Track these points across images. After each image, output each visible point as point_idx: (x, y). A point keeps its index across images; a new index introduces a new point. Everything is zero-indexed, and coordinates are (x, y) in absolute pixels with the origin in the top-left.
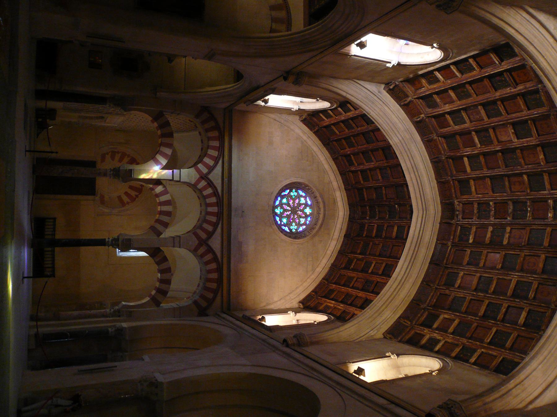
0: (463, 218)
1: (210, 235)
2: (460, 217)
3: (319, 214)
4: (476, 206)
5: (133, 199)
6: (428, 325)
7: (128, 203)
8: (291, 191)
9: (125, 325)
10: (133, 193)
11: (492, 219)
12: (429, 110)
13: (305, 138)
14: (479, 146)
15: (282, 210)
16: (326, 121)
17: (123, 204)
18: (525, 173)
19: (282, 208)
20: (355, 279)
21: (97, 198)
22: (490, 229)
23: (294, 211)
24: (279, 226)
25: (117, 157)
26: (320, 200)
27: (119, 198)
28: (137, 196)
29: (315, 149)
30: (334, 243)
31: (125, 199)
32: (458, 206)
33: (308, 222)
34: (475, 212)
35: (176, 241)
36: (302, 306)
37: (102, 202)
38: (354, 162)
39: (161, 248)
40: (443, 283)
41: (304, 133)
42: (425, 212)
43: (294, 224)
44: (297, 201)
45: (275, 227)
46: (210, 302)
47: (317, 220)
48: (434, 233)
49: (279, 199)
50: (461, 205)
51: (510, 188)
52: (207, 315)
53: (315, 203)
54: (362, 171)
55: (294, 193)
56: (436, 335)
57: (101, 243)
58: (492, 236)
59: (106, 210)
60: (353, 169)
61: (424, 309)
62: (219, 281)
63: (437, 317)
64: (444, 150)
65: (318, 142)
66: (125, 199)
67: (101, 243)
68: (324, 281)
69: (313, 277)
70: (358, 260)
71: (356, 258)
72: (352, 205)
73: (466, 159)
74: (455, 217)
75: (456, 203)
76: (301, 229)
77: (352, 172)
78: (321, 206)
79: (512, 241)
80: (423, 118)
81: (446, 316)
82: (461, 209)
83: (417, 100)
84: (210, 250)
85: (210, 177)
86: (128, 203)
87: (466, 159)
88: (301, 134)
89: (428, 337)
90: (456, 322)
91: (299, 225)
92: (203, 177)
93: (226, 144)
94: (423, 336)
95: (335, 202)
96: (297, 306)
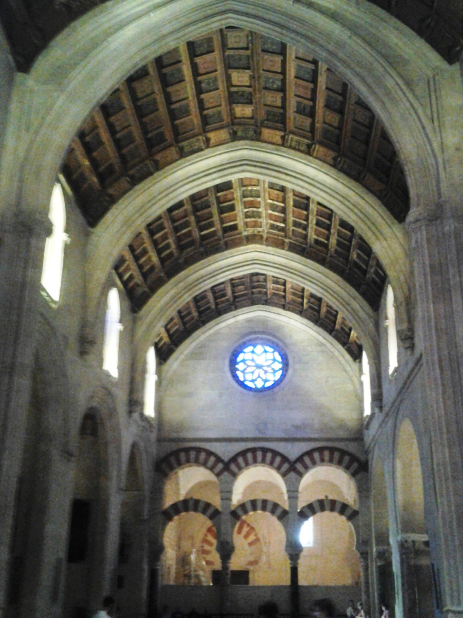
0: (261, 227)
1: (285, 459)
2: (260, 229)
3: (262, 339)
4: (248, 220)
5: (252, 529)
6: (365, 272)
7: (256, 535)
8: (237, 370)
9: (374, 549)
10: (245, 529)
11: (260, 210)
12: (157, 270)
13: (182, 357)
14: (190, 228)
15: (259, 380)
16: (166, 339)
17: (257, 540)
18: (215, 194)
19: (255, 380)
20: (329, 309)
21: (251, 568)
22: (270, 212)
23: (259, 367)
24: (277, 383)
25: (207, 547)
26: (247, 338)
27: (250, 544)
28: (248, 525)
29: (193, 345)
30: (292, 322)
31: (252, 538)
32: (250, 231)
33: (272, 350)
34: (253, 219)
35: (293, 494)
36: (358, 361)
37: (255, 563)
38: (207, 306)
39: (299, 511)
40: (325, 250)
41: (177, 359)
42: (256, 262)
43: (273, 366)
44: (249, 363)
45: (276, 389)
46: (354, 458)
47: (269, 340)
48: (277, 253)
49: (246, 383)
50: (248, 229)
51: (230, 201)
52: (367, 462)
53: (250, 343)
54: (216, 298)
55: (240, 367)
56: (372, 270)
57: (294, 571)
58: (278, 212)
59: (264, 558)
60: (213, 307)
61: (350, 269)
62: (332, 450)
63: (355, 263)
64: (195, 249)
65: (187, 341)
66: (252, 538)
67: (294, 571)
68: (333, 334)
69: (328, 345)
70: (309, 302)
71: (307, 303)
72: (253, 303)
73: (203, 233)
74: (261, 233)
75: (245, 234)
76: (279, 358)
77: (216, 307)
78: (254, 336)
79: (280, 199)
80: (165, 274)
81: (355, 256)
82: (253, 229)
83: (148, 282)
84: (300, 459)
85: (226, 459)
86: (256, 535)
87: (203, 233)
88: (179, 361)
89: (374, 276)
90: (360, 252)
91: (274, 360)
92: (227, 467)
93: (193, 444)
94: (373, 279)
95: (249, 321)
96: (358, 364)
